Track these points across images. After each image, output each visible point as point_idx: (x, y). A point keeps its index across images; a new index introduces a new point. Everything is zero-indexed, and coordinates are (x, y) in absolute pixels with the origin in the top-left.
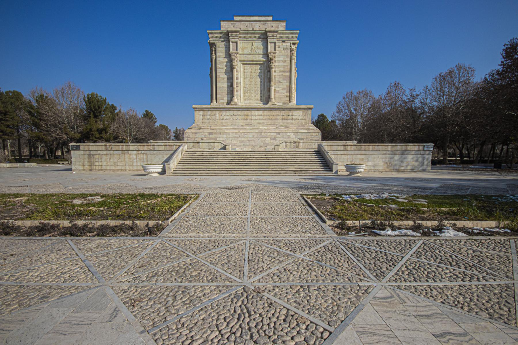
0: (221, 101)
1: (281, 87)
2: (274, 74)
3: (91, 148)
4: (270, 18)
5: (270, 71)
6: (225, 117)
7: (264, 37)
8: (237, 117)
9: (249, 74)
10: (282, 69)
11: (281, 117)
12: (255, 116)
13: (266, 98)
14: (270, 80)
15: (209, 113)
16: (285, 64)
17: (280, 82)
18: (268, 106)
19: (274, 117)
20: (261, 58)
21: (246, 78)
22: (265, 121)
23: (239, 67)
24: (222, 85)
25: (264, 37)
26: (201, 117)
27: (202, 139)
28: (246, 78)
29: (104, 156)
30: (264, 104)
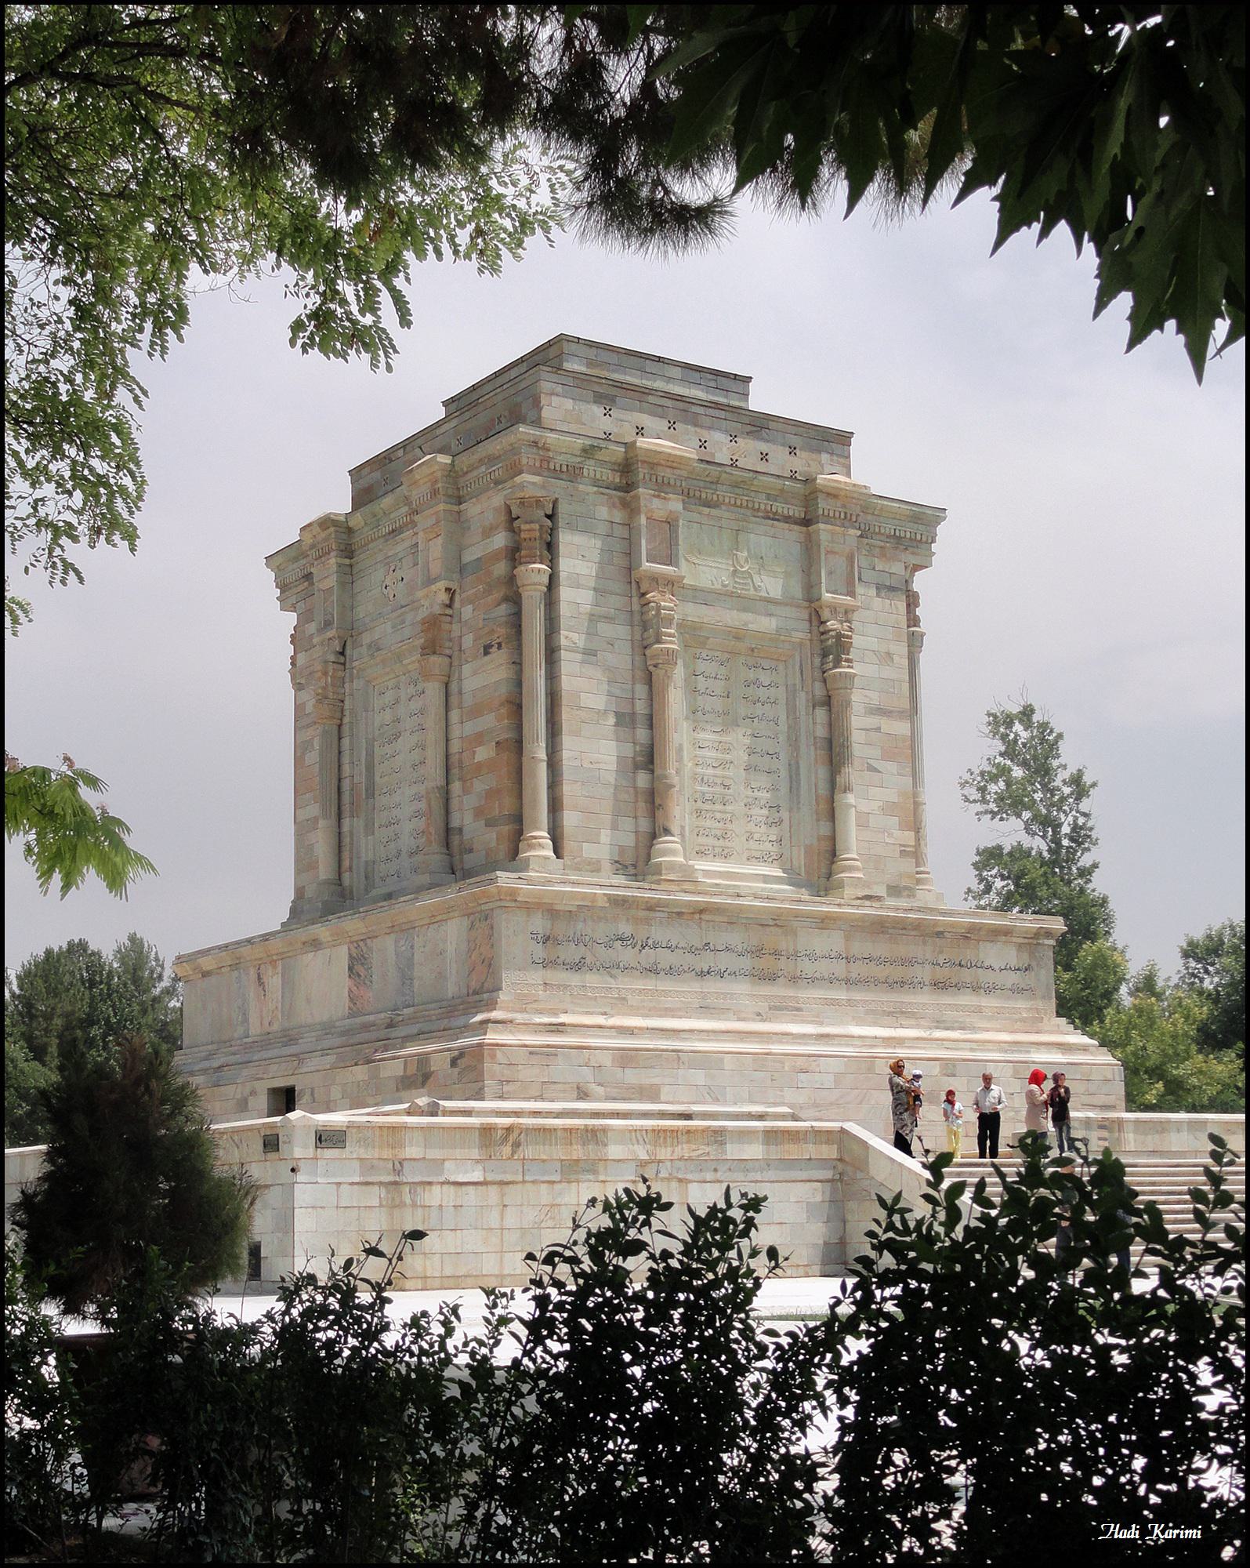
0: (589, 851)
6: (665, 958)
8: (724, 961)
9: (718, 704)
10: (875, 698)
11: (924, 973)
12: (812, 957)
14: (834, 752)
16: (887, 672)
17: (872, 769)
19: (897, 972)
22: (857, 996)
24: (593, 753)
26: (539, 952)
29: (471, 1195)
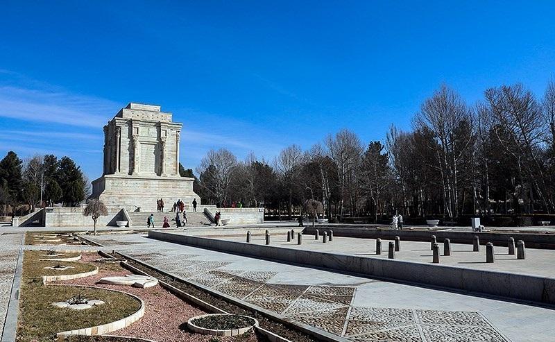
1: (170, 162)
2: (165, 153)
3: (61, 211)
4: (159, 108)
5: (162, 150)
7: (158, 125)
13: (159, 171)
14: (162, 157)
15: (117, 181)
18: (161, 177)
20: (155, 140)
21: (145, 154)
23: (138, 146)
24: (125, 158)
25: (158, 125)
27: (113, 202)
28: (145, 154)
30: (157, 175)
